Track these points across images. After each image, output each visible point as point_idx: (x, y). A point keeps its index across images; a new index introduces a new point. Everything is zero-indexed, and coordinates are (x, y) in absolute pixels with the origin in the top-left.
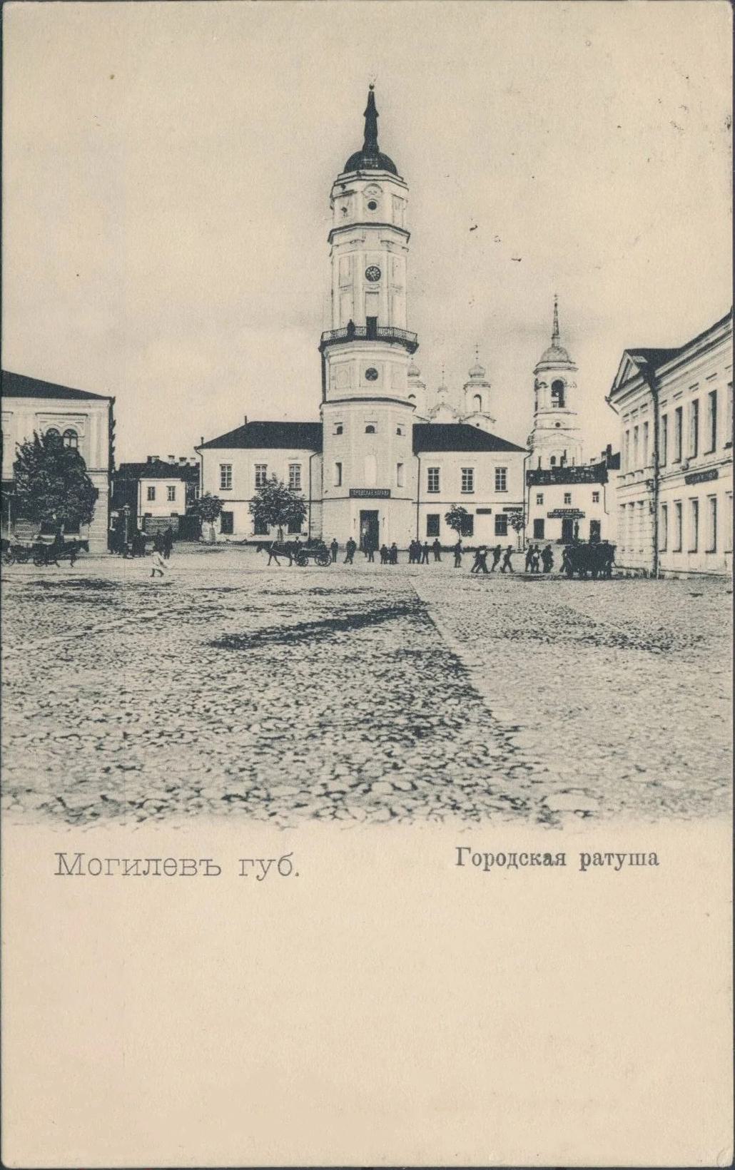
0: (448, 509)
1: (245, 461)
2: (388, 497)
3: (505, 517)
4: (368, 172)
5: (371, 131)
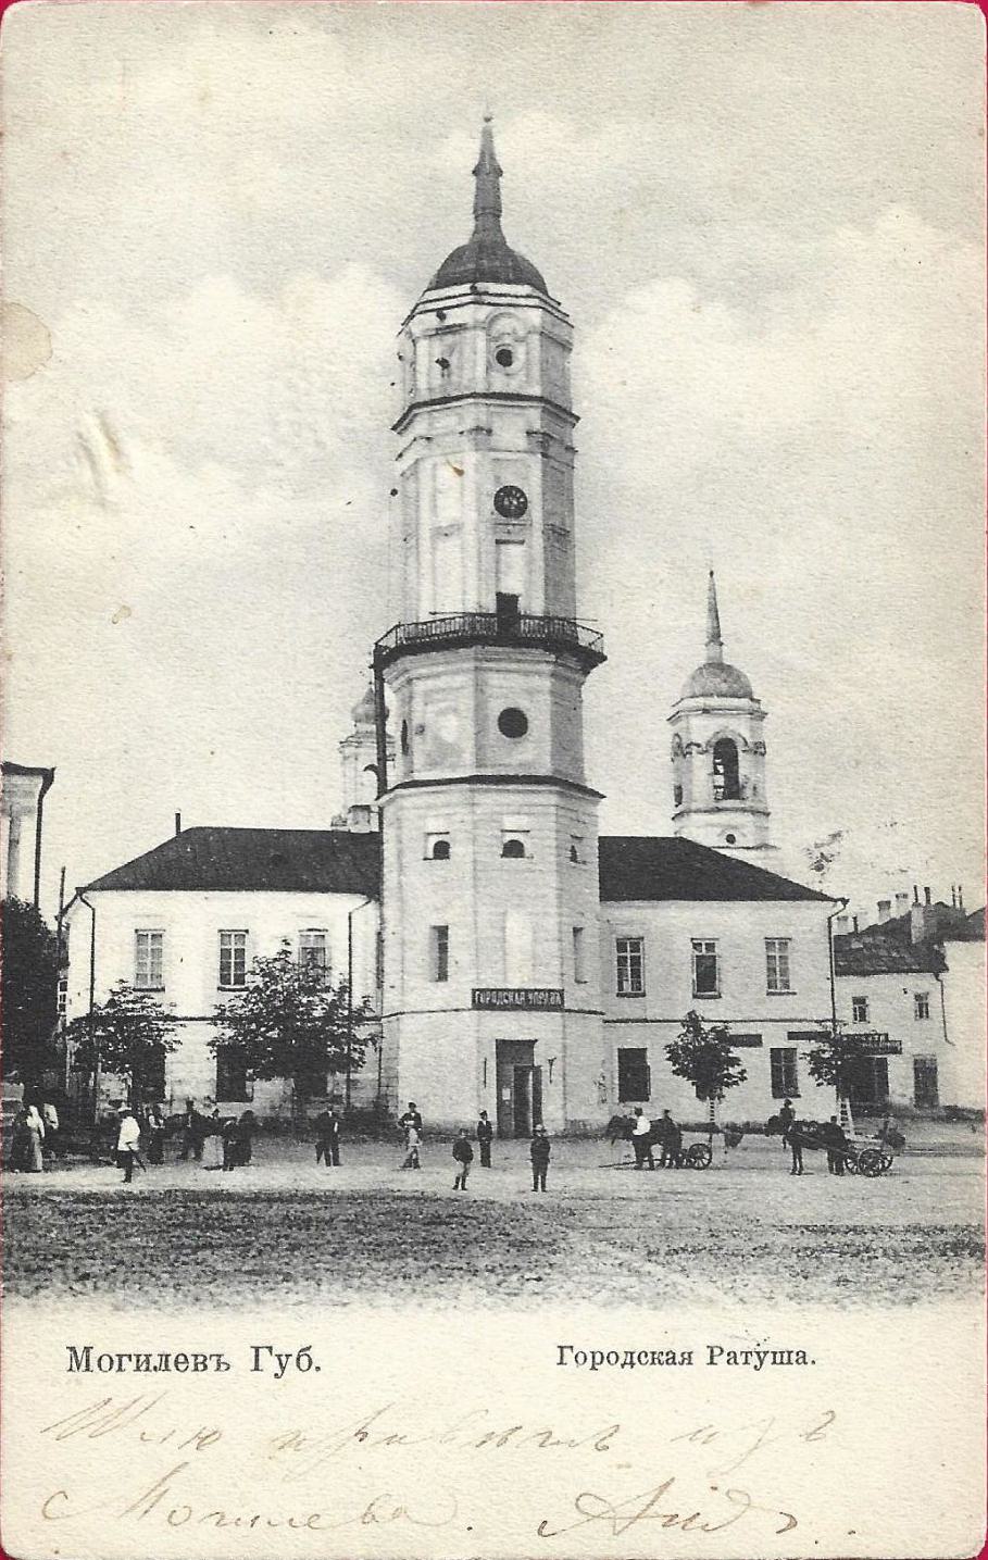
0: (675, 1034)
1: (194, 921)
2: (558, 1008)
3: (790, 1053)
4: (493, 288)
5: (488, 209)
